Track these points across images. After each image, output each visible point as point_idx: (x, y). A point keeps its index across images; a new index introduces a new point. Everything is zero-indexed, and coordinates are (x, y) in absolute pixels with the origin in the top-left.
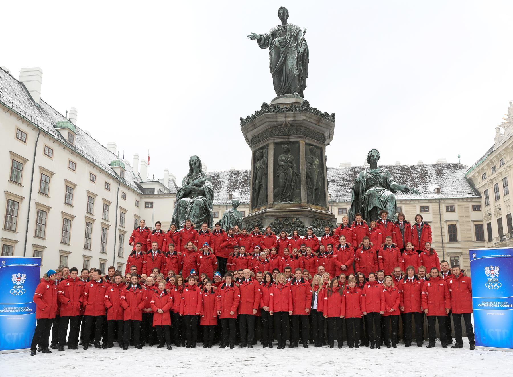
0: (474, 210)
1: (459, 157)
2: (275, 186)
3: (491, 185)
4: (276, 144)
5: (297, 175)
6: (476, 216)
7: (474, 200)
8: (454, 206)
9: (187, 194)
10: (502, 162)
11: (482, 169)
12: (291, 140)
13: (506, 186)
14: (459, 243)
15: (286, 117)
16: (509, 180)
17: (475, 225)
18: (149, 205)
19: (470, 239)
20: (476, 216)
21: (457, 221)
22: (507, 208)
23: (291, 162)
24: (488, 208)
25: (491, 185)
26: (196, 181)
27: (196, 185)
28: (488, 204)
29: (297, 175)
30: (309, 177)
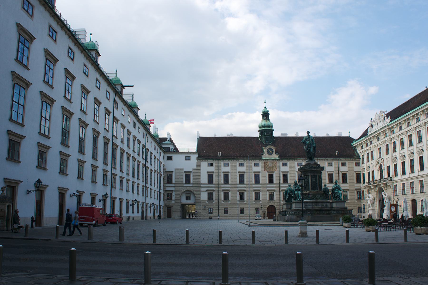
0: (356, 165)
1: (349, 133)
2: (311, 186)
3: (365, 153)
4: (311, 175)
5: (316, 184)
6: (357, 169)
7: (356, 160)
8: (346, 163)
9: (296, 190)
10: (371, 142)
11: (362, 143)
12: (315, 174)
13: (372, 156)
14: (348, 184)
15: (314, 169)
16: (374, 152)
17: (356, 174)
18: (170, 158)
19: (353, 182)
20: (357, 169)
21: (347, 172)
22: (372, 167)
23: (315, 180)
24: (363, 165)
25: (365, 153)
26: (297, 187)
27: (297, 188)
28: (363, 163)
29: (317, 184)
30: (319, 184)
